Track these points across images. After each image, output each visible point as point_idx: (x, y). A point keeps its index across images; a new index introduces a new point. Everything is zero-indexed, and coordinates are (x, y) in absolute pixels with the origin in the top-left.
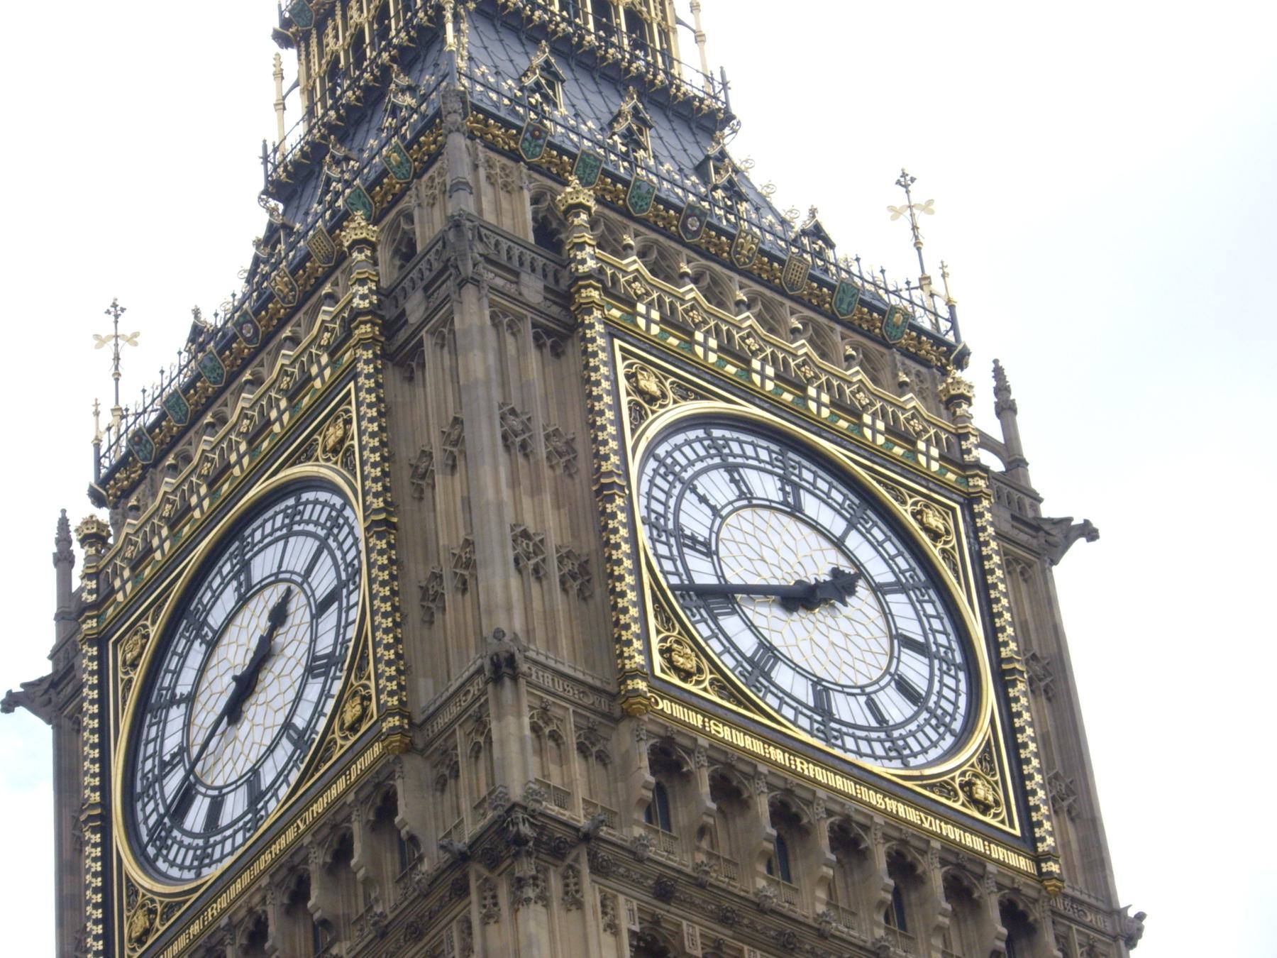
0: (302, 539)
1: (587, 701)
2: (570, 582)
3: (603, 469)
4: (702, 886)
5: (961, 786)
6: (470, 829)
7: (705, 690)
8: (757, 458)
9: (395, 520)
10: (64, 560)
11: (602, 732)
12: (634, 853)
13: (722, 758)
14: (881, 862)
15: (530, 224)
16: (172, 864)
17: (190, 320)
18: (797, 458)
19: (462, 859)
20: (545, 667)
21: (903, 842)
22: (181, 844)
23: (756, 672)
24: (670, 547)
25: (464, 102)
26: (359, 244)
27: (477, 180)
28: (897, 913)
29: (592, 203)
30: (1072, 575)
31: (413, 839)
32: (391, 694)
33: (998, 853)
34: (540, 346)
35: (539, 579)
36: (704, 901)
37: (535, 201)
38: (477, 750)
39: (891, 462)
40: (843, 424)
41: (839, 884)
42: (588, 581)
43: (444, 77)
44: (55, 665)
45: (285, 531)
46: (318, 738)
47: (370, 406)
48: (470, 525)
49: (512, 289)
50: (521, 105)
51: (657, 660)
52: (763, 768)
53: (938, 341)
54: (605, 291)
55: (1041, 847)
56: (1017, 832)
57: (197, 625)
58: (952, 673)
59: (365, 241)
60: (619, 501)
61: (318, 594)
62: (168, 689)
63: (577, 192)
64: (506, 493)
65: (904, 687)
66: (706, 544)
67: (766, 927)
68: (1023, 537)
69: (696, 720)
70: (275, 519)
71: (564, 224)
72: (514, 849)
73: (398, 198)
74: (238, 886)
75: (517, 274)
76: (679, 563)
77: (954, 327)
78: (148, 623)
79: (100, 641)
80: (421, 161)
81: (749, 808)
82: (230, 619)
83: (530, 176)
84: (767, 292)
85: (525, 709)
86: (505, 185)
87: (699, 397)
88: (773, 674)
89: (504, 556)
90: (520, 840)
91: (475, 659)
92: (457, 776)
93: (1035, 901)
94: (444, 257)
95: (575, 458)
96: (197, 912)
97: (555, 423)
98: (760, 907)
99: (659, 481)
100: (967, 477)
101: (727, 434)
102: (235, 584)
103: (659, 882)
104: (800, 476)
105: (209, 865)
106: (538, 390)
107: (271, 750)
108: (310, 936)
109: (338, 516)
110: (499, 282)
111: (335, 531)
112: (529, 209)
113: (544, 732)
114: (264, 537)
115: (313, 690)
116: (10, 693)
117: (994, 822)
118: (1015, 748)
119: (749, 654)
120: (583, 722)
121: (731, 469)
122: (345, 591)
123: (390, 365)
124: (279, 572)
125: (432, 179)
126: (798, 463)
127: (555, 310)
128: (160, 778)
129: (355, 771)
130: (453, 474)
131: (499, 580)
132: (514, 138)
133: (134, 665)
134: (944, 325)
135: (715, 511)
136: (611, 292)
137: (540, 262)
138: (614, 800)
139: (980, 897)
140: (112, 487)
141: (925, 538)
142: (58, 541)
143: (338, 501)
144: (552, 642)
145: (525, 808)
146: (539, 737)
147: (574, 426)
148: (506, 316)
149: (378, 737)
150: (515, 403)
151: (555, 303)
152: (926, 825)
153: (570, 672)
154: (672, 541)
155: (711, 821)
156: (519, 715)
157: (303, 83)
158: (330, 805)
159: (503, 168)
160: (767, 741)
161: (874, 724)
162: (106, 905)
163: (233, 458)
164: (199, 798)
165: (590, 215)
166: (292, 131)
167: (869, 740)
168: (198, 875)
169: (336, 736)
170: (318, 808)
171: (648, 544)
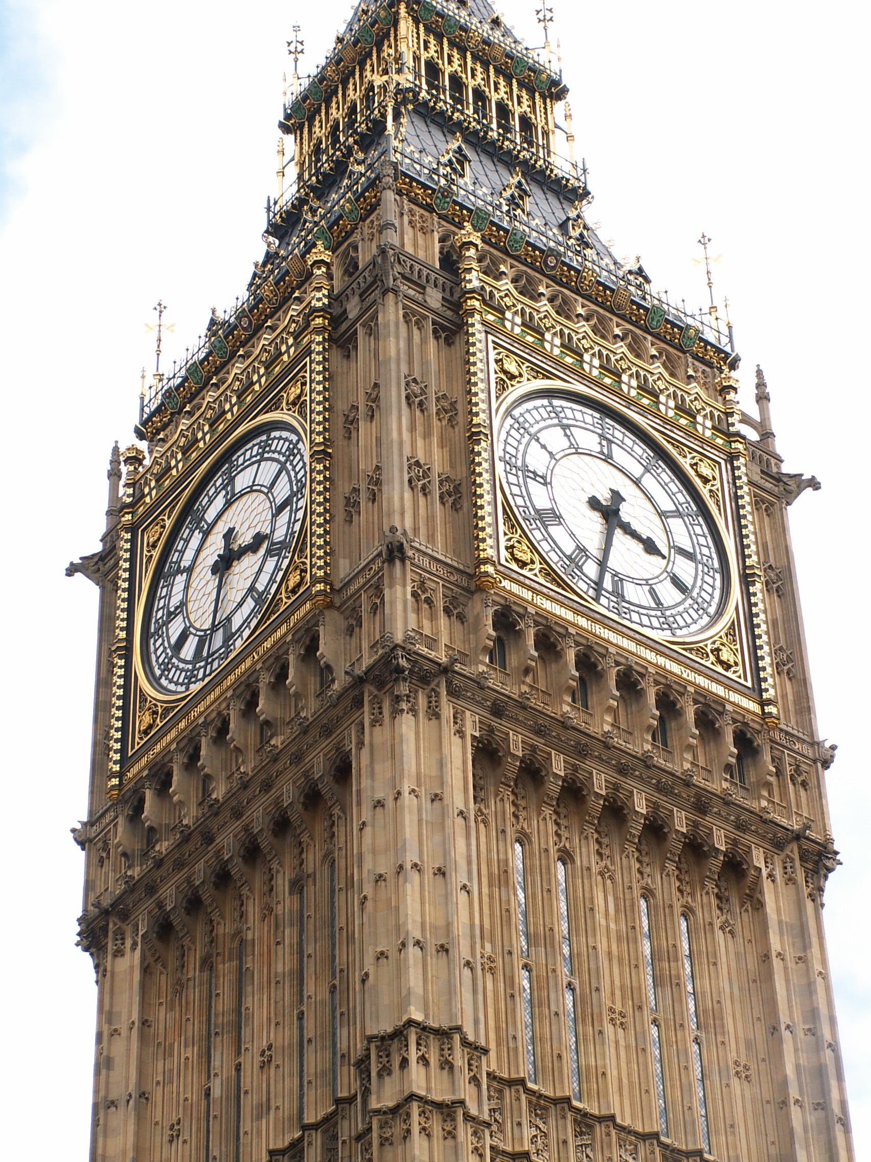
0: (269, 463)
1: (452, 579)
2: (446, 498)
3: (474, 422)
4: (524, 708)
5: (712, 651)
6: (367, 662)
7: (536, 575)
9: (330, 451)
10: (114, 474)
11: (462, 599)
12: (478, 683)
13: (544, 622)
14: (652, 699)
15: (437, 255)
16: (171, 681)
17: (210, 315)
18: (612, 423)
19: (359, 682)
20: (425, 554)
21: (668, 686)
22: (177, 668)
23: (573, 565)
25: (396, 169)
26: (318, 263)
27: (402, 224)
28: (661, 734)
29: (479, 242)
30: (800, 513)
31: (328, 667)
32: (320, 568)
33: (734, 697)
34: (437, 338)
35: (425, 495)
36: (526, 719)
37: (442, 240)
38: (375, 609)
40: (530, 339)
41: (621, 712)
42: (460, 497)
43: (383, 153)
44: (104, 545)
45: (258, 457)
46: (270, 597)
47: (318, 373)
48: (379, 455)
49: (420, 297)
50: (436, 174)
51: (504, 554)
52: (572, 630)
53: (719, 350)
54: (484, 302)
55: (765, 696)
56: (749, 684)
57: (198, 520)
58: (711, 574)
59: (322, 261)
60: (483, 444)
61: (277, 501)
62: (175, 563)
63: (469, 233)
64: (406, 436)
65: (677, 582)
67: (568, 739)
68: (768, 485)
69: (527, 595)
70: (252, 450)
71: (460, 256)
72: (395, 676)
73: (349, 234)
75: (424, 288)
76: (523, 489)
77: (731, 341)
78: (166, 518)
79: (133, 529)
80: (365, 210)
81: (561, 657)
83: (439, 223)
84: (601, 311)
85: (409, 581)
86: (422, 228)
87: (546, 377)
89: (402, 477)
90: (399, 670)
91: (377, 547)
92: (361, 626)
93: (759, 732)
94: (374, 274)
95: (456, 414)
96: (184, 713)
97: (444, 390)
98: (564, 724)
99: (513, 432)
100: (730, 442)
102: (224, 492)
103: (494, 704)
105: (195, 682)
106: (433, 367)
107: (240, 605)
108: (258, 731)
109: (294, 448)
110: (411, 292)
111: (292, 458)
112: (437, 246)
113: (421, 597)
114: (245, 461)
115: (271, 564)
116: (72, 564)
117: (733, 677)
118: (752, 627)
120: (449, 593)
121: (565, 427)
122: (295, 499)
123: (335, 346)
124: (253, 485)
125: (372, 222)
126: (612, 426)
127: (449, 313)
128: (166, 623)
130: (371, 422)
131: (398, 493)
132: (430, 196)
133: (154, 546)
134: (724, 340)
136: (489, 303)
137: (441, 280)
138: (467, 647)
139: (681, 708)
140: (150, 427)
141: (698, 482)
142: (111, 462)
143: (294, 438)
144: (431, 538)
145: (404, 648)
146: (417, 601)
147: (457, 393)
148: (414, 316)
149: (310, 598)
150: (416, 375)
151: (449, 308)
152: (685, 676)
153: (443, 558)
154: (520, 473)
155: (534, 664)
156: (404, 586)
157: (296, 159)
158: (275, 643)
159: (421, 216)
160: (576, 612)
161: (653, 605)
162: (125, 708)
163: (227, 407)
164: (191, 636)
165: (477, 250)
166: (286, 190)
168: (187, 689)
169: (283, 596)
170: (268, 644)
171: (503, 475)
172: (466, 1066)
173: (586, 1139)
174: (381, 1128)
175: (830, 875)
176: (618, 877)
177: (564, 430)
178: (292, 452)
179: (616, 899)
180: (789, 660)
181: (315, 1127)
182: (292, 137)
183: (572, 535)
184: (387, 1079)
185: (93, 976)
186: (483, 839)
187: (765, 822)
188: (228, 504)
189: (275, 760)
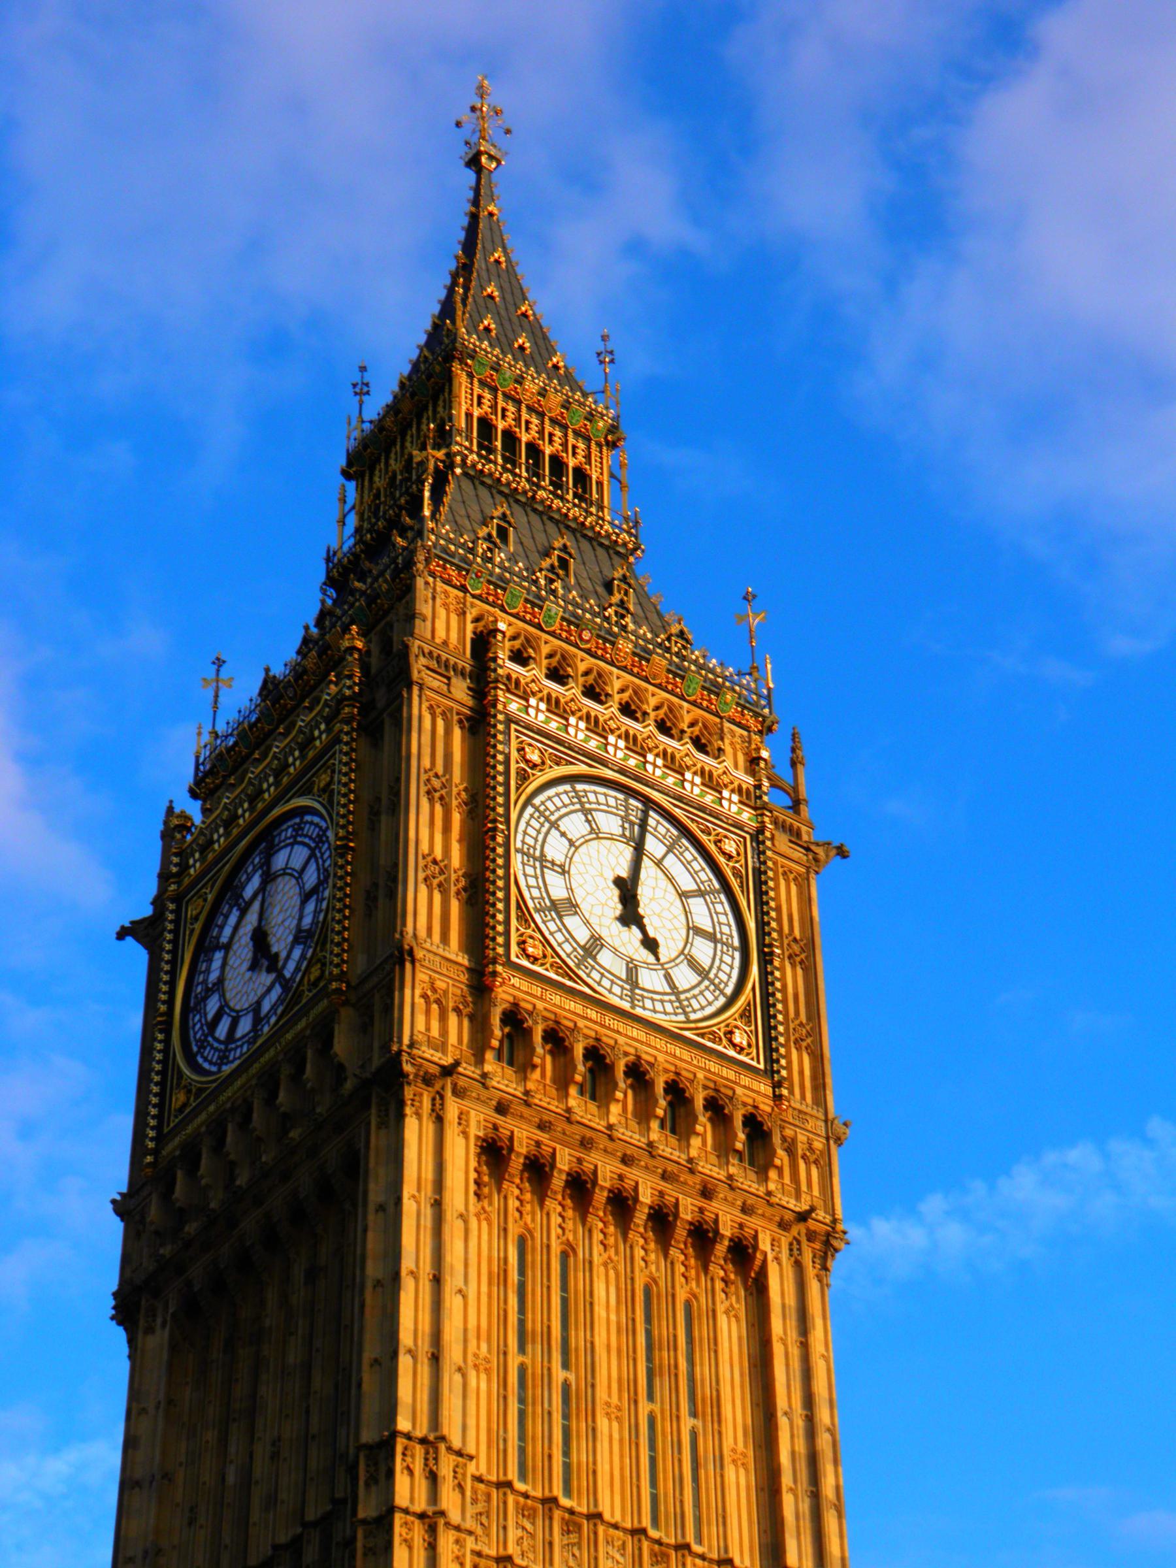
5: (725, 1034)
7: (547, 970)
20: (436, 954)
24: (535, 868)
44: (155, 910)
55: (776, 1077)
56: (762, 1066)
65: (693, 964)
66: (562, 866)
73: (386, 613)
74: (239, 1083)
75: (449, 678)
76: (540, 880)
88: (598, 957)
102: (260, 872)
103: (499, 1103)
112: (470, 627)
116: (123, 927)
119: (582, 943)
121: (586, 812)
124: (286, 868)
128: (205, 999)
129: (313, 1014)
135: (571, 843)
141: (722, 860)
152: (695, 1062)
154: (538, 864)
161: (668, 990)
164: (225, 1017)
167: (662, 1001)
170: (289, 1036)
171: (520, 866)
172: (452, 1474)
173: (573, 1538)
174: (365, 1537)
175: (837, 1255)
177: (586, 816)
178: (321, 839)
181: (314, 1524)
183: (587, 923)
184: (374, 1488)
185: (125, 1350)
186: (485, 1237)
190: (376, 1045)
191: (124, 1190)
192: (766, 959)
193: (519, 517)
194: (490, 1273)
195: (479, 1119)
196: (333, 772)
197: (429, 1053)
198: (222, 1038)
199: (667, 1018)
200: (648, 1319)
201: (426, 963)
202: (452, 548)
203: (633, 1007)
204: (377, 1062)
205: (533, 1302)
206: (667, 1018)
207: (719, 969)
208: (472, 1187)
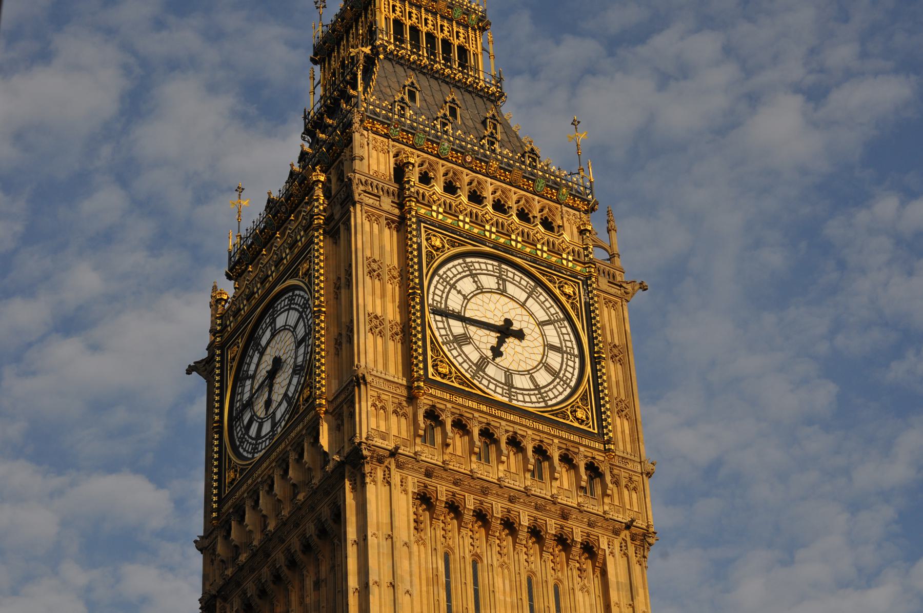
8: (487, 270)
39: (550, 266)
55: (606, 438)
56: (596, 431)
65: (549, 369)
68: (613, 291)
70: (283, 302)
73: (339, 155)
82: (268, 343)
101: (473, 260)
104: (507, 276)
112: (392, 160)
120: (397, 401)
121: (473, 276)
132: (386, 128)
135: (465, 297)
141: (563, 299)
161: (533, 387)
170: (293, 435)
176: (512, 567)
179: (510, 581)
180: (627, 407)
182: (319, 66)
186: (423, 555)
187: (607, 520)
188: (273, 336)
189: (300, 509)
190: (346, 439)
191: (202, 534)
192: (595, 361)
193: (424, 82)
194: (427, 579)
195: (413, 483)
196: (310, 262)
197: (378, 442)
198: (254, 436)
199: (533, 405)
200: (531, 599)
201: (374, 384)
202: (378, 110)
203: (511, 400)
204: (347, 449)
205: (456, 594)
206: (533, 405)
207: (566, 370)
208: (412, 525)
